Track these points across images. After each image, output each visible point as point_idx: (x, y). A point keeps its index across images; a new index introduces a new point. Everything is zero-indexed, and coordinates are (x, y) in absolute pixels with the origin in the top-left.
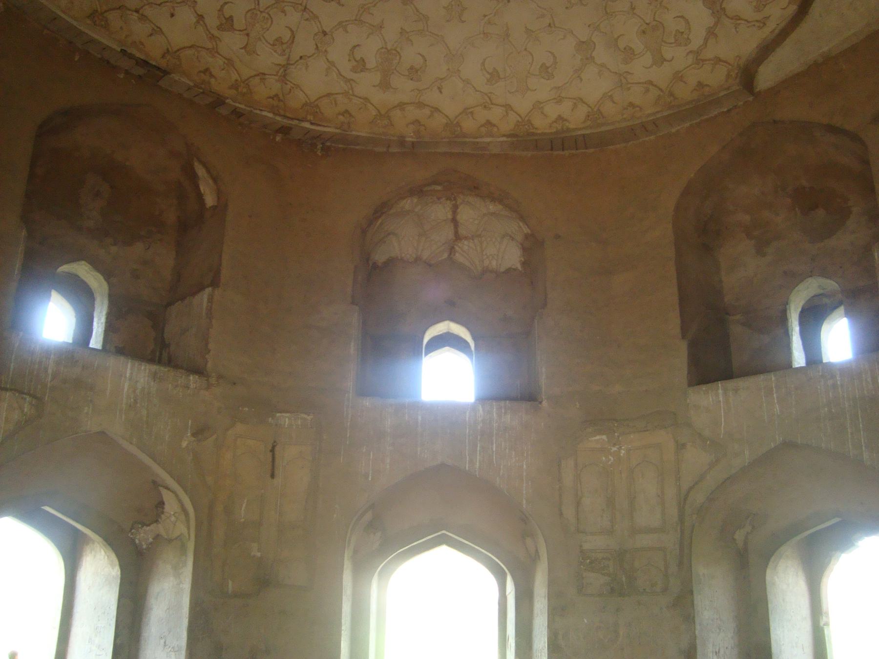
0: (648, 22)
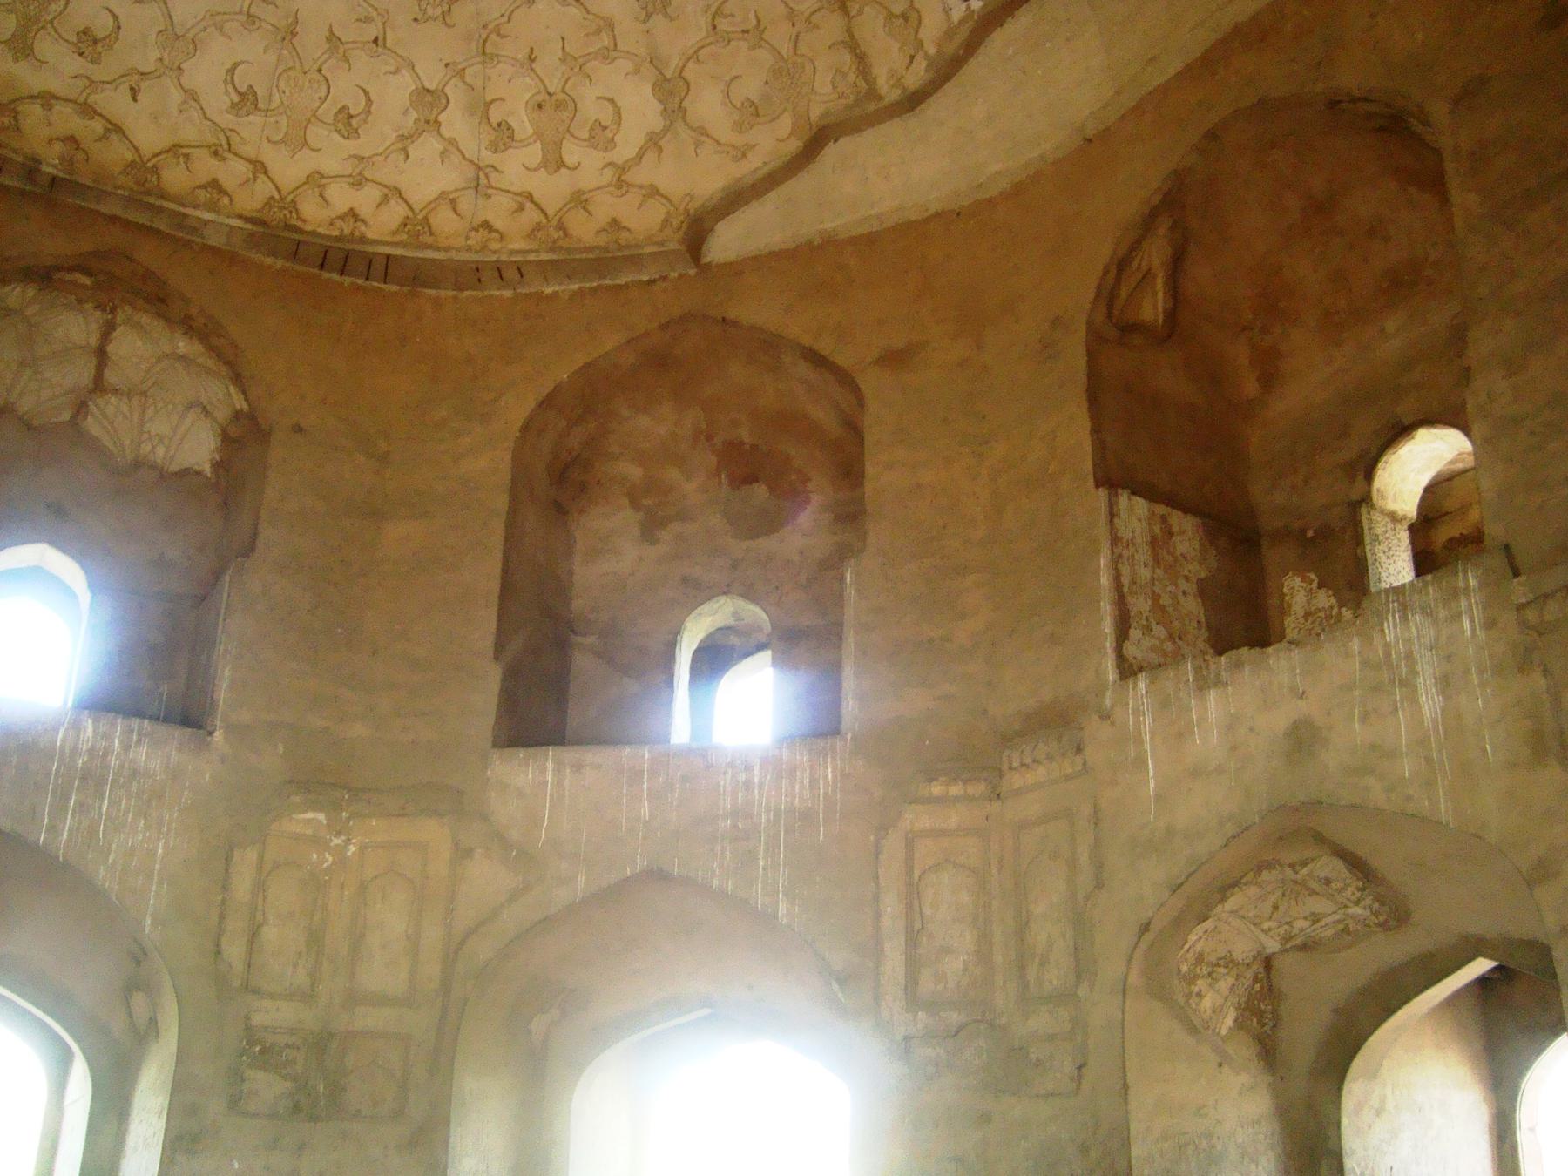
0: (551, 90)
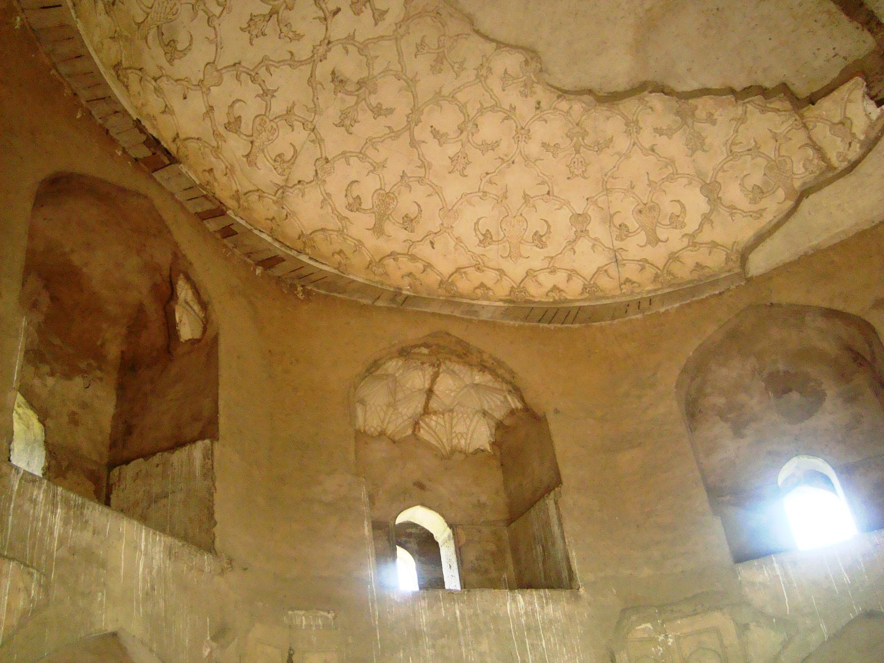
0: (645, 202)
